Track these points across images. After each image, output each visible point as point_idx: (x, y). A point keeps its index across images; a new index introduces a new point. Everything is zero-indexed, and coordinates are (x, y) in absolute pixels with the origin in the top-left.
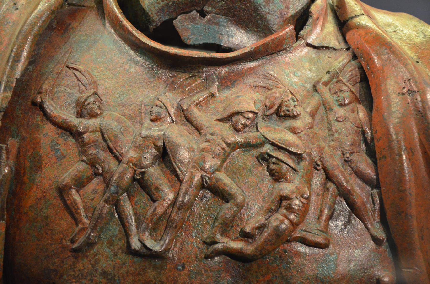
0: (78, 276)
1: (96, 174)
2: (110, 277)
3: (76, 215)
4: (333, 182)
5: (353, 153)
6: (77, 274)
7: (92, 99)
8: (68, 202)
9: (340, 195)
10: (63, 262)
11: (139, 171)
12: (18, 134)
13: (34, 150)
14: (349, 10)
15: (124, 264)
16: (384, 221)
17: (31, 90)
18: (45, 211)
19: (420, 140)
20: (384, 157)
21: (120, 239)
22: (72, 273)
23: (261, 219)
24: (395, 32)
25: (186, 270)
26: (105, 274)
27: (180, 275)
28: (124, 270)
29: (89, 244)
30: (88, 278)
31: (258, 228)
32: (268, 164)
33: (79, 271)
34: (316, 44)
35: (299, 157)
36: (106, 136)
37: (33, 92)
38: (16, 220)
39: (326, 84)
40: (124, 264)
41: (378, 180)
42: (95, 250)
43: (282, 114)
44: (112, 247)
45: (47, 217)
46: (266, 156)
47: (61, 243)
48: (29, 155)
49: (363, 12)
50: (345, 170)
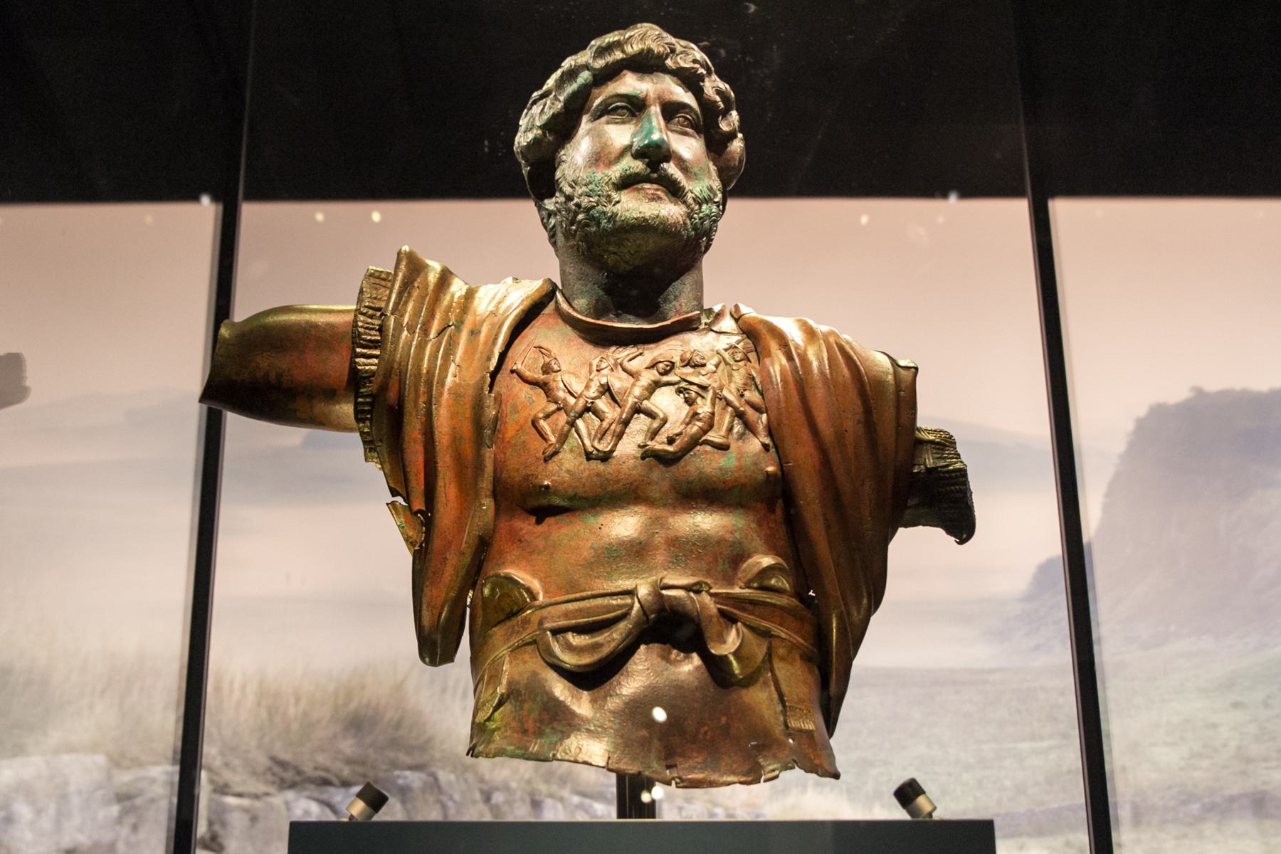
1: (559, 409)
3: (546, 436)
4: (731, 406)
8: (539, 428)
9: (737, 416)
10: (537, 468)
11: (590, 401)
15: (581, 463)
16: (770, 432)
19: (793, 377)
22: (544, 473)
26: (568, 471)
28: (582, 467)
29: (556, 453)
31: (677, 435)
32: (684, 395)
35: (704, 388)
40: (581, 463)
41: (766, 407)
43: (693, 364)
45: (524, 442)
46: (682, 390)
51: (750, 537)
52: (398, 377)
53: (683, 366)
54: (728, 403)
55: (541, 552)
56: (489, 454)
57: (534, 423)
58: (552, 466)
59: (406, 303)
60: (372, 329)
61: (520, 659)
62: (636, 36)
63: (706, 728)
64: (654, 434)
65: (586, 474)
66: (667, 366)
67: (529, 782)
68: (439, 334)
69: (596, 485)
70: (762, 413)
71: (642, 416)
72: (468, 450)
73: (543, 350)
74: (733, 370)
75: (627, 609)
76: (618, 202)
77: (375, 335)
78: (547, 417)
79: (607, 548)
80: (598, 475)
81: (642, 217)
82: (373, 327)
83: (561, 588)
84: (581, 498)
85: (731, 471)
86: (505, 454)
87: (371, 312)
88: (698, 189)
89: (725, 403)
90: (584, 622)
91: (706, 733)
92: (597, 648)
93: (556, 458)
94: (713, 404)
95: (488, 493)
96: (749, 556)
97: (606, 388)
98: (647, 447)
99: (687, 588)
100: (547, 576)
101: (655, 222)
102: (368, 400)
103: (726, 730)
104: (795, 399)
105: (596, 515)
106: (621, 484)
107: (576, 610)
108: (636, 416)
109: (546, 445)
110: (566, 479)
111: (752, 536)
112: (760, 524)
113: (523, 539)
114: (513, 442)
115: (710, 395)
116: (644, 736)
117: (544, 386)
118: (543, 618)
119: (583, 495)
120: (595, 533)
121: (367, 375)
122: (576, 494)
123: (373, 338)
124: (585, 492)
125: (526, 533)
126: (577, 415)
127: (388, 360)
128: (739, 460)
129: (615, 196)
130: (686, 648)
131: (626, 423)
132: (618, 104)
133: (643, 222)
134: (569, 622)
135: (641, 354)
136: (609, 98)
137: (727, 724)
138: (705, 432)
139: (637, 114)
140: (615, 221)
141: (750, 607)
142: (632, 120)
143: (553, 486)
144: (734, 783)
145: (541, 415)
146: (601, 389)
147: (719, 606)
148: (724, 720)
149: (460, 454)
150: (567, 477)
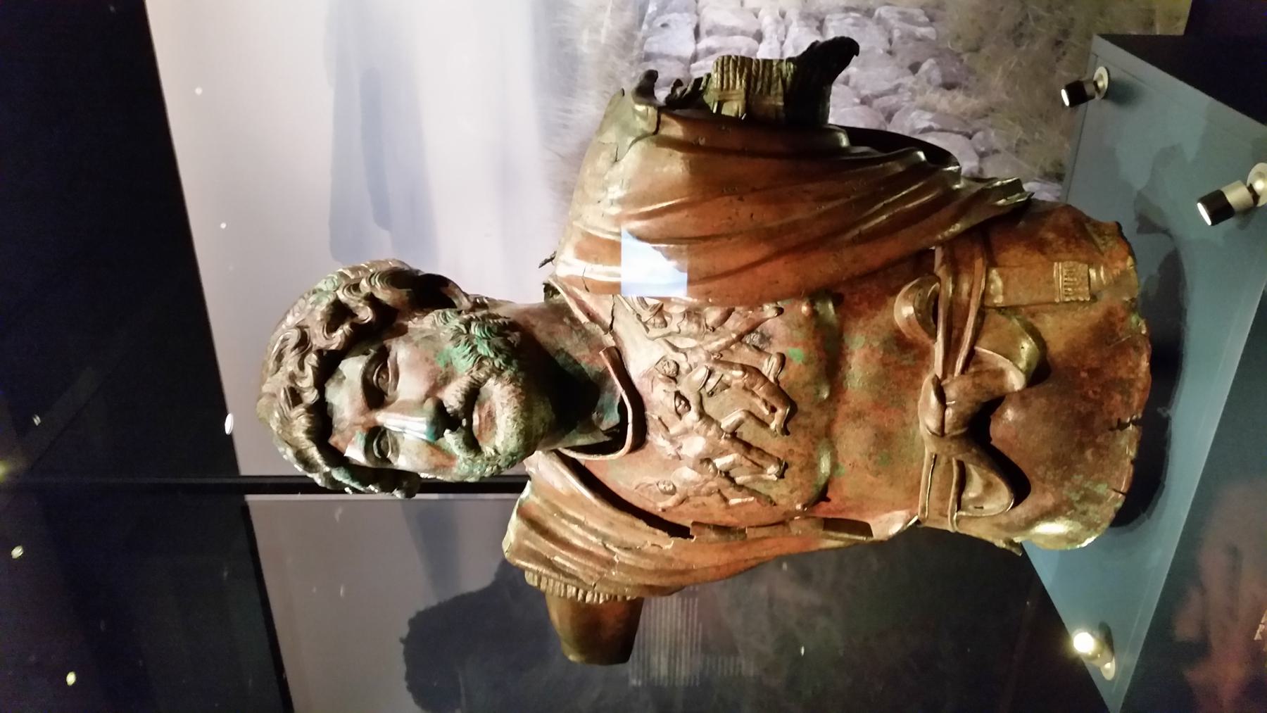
51: (875, 329)
63: (1090, 392)
64: (764, 424)
67: (631, 63)
96: (898, 331)
103: (1094, 372)
111: (874, 326)
128: (796, 345)
138: (766, 379)
141: (955, 333)
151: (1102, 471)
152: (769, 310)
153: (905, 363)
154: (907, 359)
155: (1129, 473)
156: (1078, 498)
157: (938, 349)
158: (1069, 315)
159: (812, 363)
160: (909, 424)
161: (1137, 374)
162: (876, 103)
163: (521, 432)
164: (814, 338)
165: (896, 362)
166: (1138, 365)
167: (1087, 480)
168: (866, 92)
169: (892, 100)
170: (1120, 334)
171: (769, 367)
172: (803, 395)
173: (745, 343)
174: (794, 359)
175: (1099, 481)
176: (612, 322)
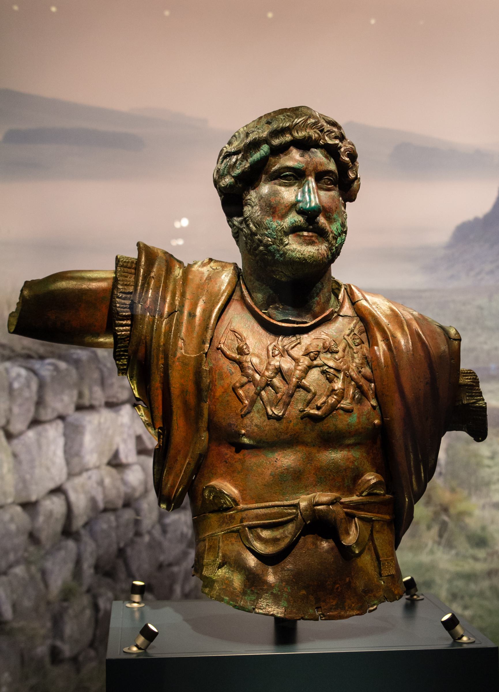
0: (245, 426)
1: (249, 382)
2: (259, 427)
3: (242, 400)
4: (354, 382)
5: (363, 368)
6: (244, 425)
7: (245, 347)
8: (238, 394)
9: (357, 387)
10: (237, 420)
12: (211, 363)
13: (219, 370)
14: (356, 297)
17: (215, 342)
18: (227, 398)
19: (392, 362)
20: (376, 370)
21: (262, 410)
22: (242, 425)
23: (323, 399)
24: (377, 308)
25: (292, 422)
26: (256, 425)
27: (290, 425)
29: (249, 412)
30: (249, 427)
33: (245, 424)
34: (343, 315)
35: (338, 371)
36: (253, 364)
37: (216, 343)
38: (213, 402)
39: (348, 335)
41: (374, 379)
42: (251, 415)
43: (331, 351)
44: (259, 414)
45: (228, 401)
46: (325, 372)
47: (235, 412)
48: (217, 372)
49: (362, 298)
50: (359, 375)
51: (363, 463)
52: (144, 345)
53: (325, 352)
54: (352, 379)
55: (240, 472)
56: (206, 406)
57: (234, 389)
58: (247, 421)
59: (147, 291)
60: (125, 308)
61: (229, 541)
62: (300, 123)
63: (338, 586)
65: (267, 428)
66: (316, 354)
68: (169, 316)
69: (274, 435)
70: (372, 382)
71: (301, 390)
72: (192, 400)
73: (237, 334)
74: (354, 353)
75: (293, 516)
76: (287, 244)
77: (127, 312)
78: (242, 386)
79: (280, 476)
80: (275, 429)
81: (303, 258)
82: (126, 306)
83: (253, 498)
84: (264, 442)
85: (354, 426)
86: (215, 406)
87: (124, 296)
88: (335, 229)
89: (350, 379)
90: (268, 523)
91: (337, 588)
92: (277, 541)
93: (249, 416)
94: (343, 382)
95: (205, 429)
96: (362, 475)
97: (279, 370)
98: (305, 412)
99: (328, 504)
100: (245, 490)
101: (311, 261)
102: (127, 357)
104: (392, 376)
105: (273, 452)
106: (289, 435)
107: (263, 515)
108: (297, 390)
109: (241, 406)
110: (256, 430)
112: (368, 453)
113: (228, 461)
114: (220, 399)
115: (341, 376)
116: (304, 594)
117: (240, 363)
118: (243, 518)
119: (266, 441)
120: (273, 464)
121: (124, 337)
122: (261, 440)
123: (127, 314)
124: (267, 439)
125: (229, 457)
126: (262, 389)
127: (138, 336)
128: (358, 418)
129: (285, 240)
130: (326, 537)
131: (291, 396)
132: (288, 173)
133: (303, 261)
134: (259, 522)
135: (299, 343)
136: (282, 168)
137: (350, 582)
138: (339, 402)
139: (299, 178)
140: (285, 257)
142: (295, 183)
143: (247, 434)
144: (353, 615)
145: (238, 385)
146: (276, 371)
147: (345, 510)
148: (347, 580)
149: (186, 401)
150: (256, 429)
151: (295, 602)
152: (374, 402)
153: (346, 480)
154: (348, 482)
155: (296, 617)
156: (275, 592)
157: (355, 498)
158: (372, 568)
159: (348, 428)
160: (306, 489)
161: (348, 610)
162: (120, 562)
163: (305, 259)
164: (362, 428)
165: (347, 476)
166: (353, 610)
167: (288, 594)
168: (129, 551)
169: (122, 575)
170: (367, 597)
171: (345, 404)
172: (327, 425)
173: (356, 390)
174: (351, 418)
175: (288, 601)
176: (341, 316)
